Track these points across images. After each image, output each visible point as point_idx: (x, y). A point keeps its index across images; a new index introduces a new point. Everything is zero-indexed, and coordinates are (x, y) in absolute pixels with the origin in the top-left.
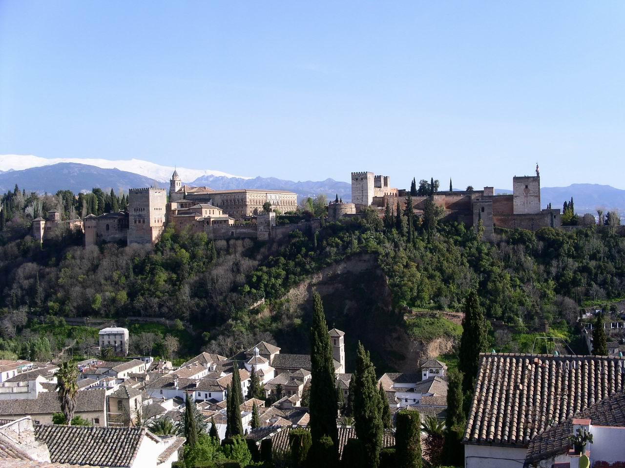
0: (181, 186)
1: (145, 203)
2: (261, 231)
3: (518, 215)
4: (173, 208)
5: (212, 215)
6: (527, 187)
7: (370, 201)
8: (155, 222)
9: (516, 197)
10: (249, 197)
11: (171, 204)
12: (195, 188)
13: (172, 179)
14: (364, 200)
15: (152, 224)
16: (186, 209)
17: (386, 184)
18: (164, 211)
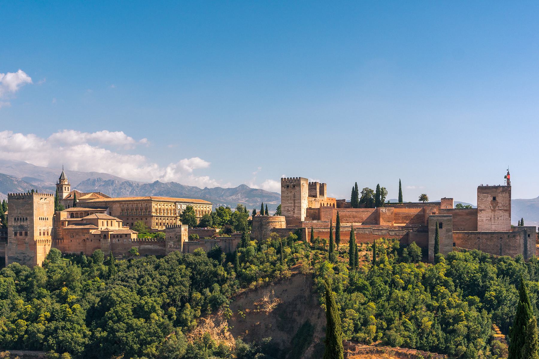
0: (69, 191)
1: (28, 212)
2: (170, 247)
4: (62, 219)
5: (110, 228)
6: (494, 199)
8: (40, 235)
9: (481, 210)
10: (155, 206)
11: (60, 213)
13: (58, 183)
14: (296, 212)
17: (322, 193)
18: (50, 222)
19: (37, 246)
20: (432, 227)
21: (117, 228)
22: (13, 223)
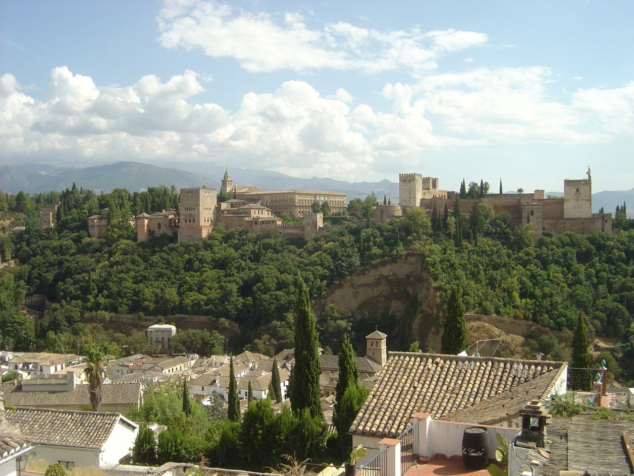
3: (568, 219)
4: (222, 208)
5: (260, 216)
6: (578, 190)
7: (418, 204)
9: (567, 200)
12: (245, 188)
14: (412, 202)
15: (202, 223)
16: (236, 209)
17: (434, 186)
19: (203, 231)
20: (525, 214)
21: (267, 216)
22: (184, 212)
